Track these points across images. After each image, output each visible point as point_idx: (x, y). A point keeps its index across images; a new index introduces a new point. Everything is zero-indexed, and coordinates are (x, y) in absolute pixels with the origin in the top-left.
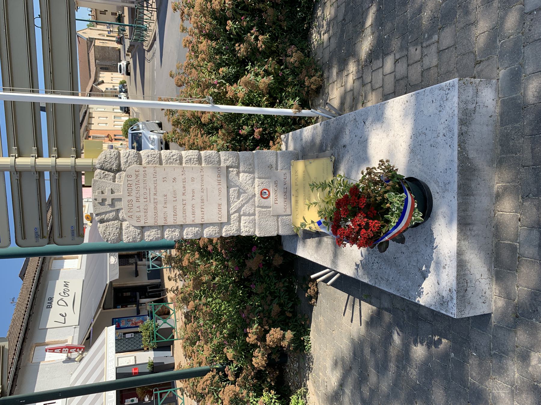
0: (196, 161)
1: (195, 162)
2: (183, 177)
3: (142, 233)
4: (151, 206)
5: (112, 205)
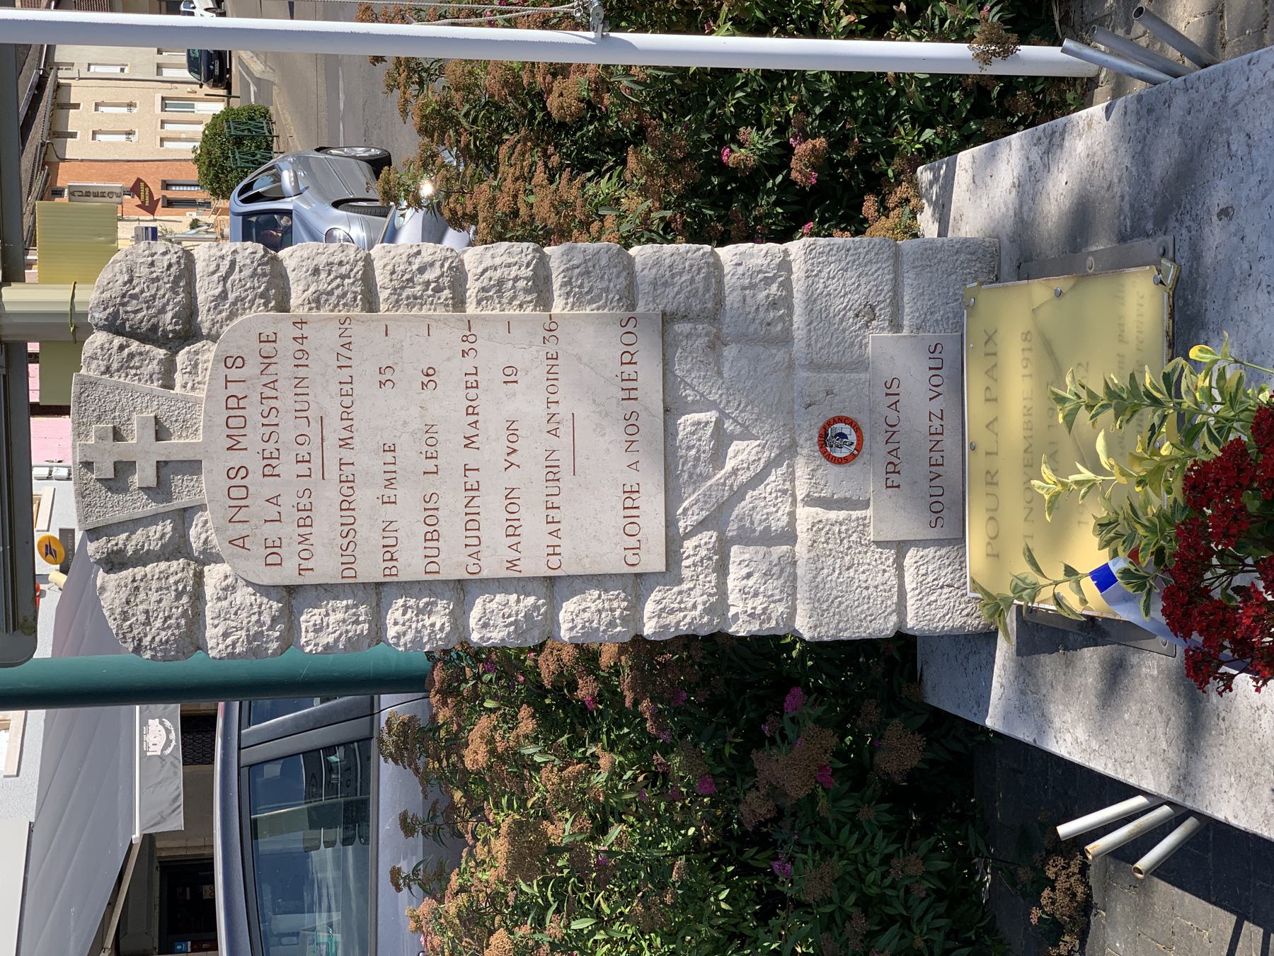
0: (527, 291)
1: (521, 297)
2: (468, 364)
3: (289, 617)
4: (327, 497)
5: (161, 490)
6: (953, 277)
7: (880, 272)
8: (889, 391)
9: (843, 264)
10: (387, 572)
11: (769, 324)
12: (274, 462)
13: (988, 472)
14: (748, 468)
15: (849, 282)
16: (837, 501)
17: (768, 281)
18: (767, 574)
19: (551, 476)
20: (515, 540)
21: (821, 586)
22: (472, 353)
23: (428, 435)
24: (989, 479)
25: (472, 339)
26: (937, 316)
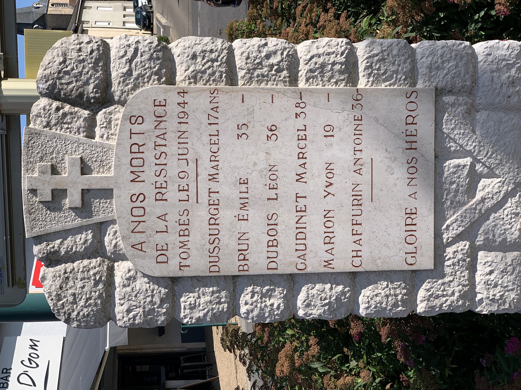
0: (341, 72)
1: (337, 76)
2: (300, 123)
3: (172, 299)
4: (200, 216)
5: (84, 209)
10: (241, 268)
11: (509, 97)
12: (163, 191)
14: (492, 198)
17: (509, 67)
18: (504, 272)
19: (356, 202)
20: (331, 246)
22: (302, 115)
23: (271, 173)
25: (302, 105)
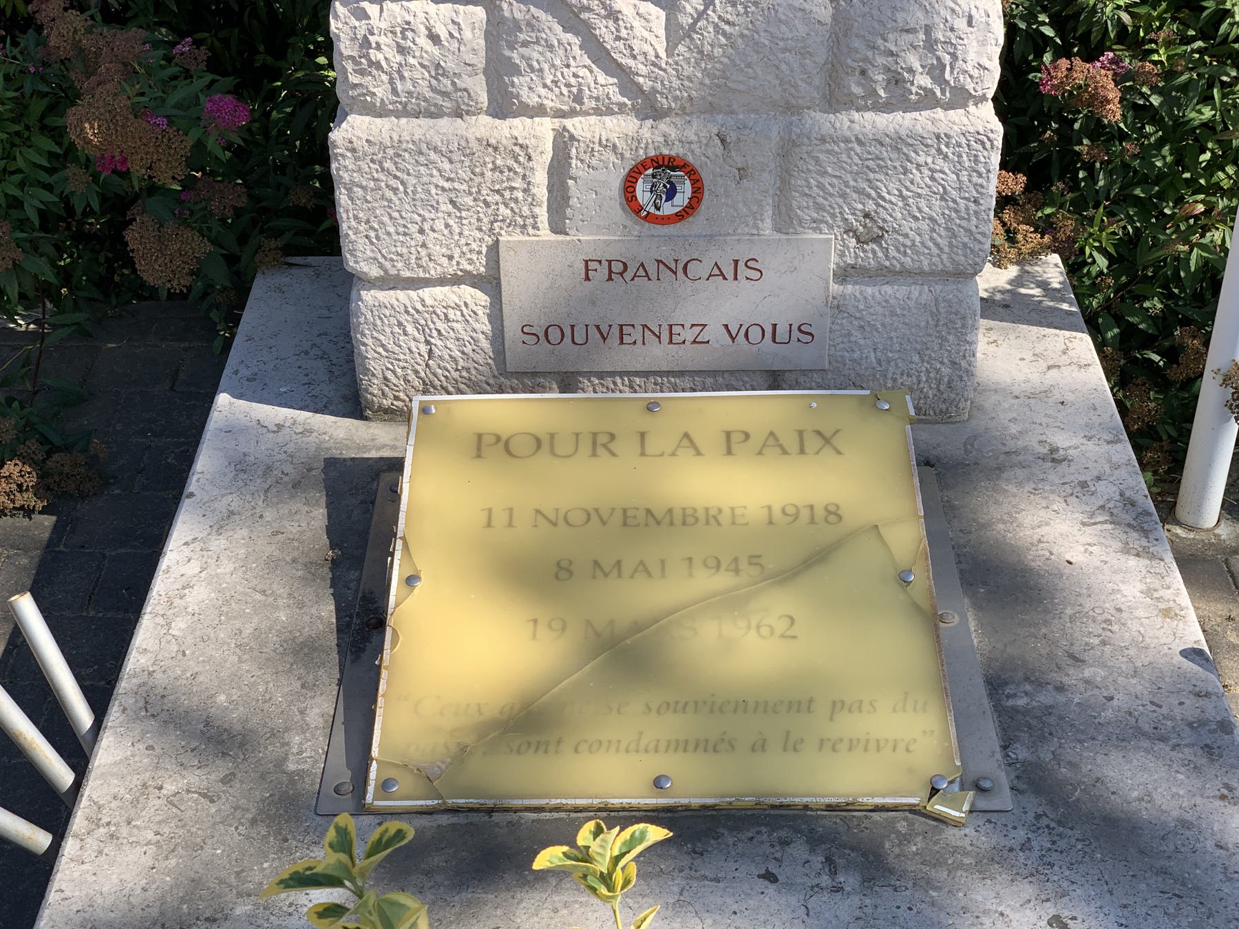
6: (916, 358)
7: (935, 251)
8: (741, 265)
9: (954, 194)
11: (863, 73)
13: (612, 437)
14: (618, 38)
15: (923, 203)
16: (564, 188)
17: (936, 71)
18: (438, 70)
21: (422, 159)
24: (603, 439)
26: (857, 336)
